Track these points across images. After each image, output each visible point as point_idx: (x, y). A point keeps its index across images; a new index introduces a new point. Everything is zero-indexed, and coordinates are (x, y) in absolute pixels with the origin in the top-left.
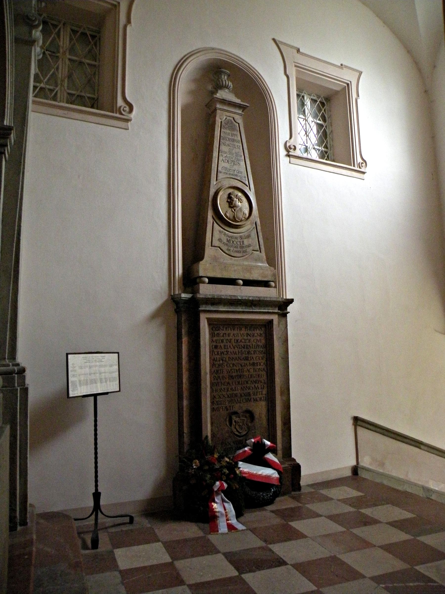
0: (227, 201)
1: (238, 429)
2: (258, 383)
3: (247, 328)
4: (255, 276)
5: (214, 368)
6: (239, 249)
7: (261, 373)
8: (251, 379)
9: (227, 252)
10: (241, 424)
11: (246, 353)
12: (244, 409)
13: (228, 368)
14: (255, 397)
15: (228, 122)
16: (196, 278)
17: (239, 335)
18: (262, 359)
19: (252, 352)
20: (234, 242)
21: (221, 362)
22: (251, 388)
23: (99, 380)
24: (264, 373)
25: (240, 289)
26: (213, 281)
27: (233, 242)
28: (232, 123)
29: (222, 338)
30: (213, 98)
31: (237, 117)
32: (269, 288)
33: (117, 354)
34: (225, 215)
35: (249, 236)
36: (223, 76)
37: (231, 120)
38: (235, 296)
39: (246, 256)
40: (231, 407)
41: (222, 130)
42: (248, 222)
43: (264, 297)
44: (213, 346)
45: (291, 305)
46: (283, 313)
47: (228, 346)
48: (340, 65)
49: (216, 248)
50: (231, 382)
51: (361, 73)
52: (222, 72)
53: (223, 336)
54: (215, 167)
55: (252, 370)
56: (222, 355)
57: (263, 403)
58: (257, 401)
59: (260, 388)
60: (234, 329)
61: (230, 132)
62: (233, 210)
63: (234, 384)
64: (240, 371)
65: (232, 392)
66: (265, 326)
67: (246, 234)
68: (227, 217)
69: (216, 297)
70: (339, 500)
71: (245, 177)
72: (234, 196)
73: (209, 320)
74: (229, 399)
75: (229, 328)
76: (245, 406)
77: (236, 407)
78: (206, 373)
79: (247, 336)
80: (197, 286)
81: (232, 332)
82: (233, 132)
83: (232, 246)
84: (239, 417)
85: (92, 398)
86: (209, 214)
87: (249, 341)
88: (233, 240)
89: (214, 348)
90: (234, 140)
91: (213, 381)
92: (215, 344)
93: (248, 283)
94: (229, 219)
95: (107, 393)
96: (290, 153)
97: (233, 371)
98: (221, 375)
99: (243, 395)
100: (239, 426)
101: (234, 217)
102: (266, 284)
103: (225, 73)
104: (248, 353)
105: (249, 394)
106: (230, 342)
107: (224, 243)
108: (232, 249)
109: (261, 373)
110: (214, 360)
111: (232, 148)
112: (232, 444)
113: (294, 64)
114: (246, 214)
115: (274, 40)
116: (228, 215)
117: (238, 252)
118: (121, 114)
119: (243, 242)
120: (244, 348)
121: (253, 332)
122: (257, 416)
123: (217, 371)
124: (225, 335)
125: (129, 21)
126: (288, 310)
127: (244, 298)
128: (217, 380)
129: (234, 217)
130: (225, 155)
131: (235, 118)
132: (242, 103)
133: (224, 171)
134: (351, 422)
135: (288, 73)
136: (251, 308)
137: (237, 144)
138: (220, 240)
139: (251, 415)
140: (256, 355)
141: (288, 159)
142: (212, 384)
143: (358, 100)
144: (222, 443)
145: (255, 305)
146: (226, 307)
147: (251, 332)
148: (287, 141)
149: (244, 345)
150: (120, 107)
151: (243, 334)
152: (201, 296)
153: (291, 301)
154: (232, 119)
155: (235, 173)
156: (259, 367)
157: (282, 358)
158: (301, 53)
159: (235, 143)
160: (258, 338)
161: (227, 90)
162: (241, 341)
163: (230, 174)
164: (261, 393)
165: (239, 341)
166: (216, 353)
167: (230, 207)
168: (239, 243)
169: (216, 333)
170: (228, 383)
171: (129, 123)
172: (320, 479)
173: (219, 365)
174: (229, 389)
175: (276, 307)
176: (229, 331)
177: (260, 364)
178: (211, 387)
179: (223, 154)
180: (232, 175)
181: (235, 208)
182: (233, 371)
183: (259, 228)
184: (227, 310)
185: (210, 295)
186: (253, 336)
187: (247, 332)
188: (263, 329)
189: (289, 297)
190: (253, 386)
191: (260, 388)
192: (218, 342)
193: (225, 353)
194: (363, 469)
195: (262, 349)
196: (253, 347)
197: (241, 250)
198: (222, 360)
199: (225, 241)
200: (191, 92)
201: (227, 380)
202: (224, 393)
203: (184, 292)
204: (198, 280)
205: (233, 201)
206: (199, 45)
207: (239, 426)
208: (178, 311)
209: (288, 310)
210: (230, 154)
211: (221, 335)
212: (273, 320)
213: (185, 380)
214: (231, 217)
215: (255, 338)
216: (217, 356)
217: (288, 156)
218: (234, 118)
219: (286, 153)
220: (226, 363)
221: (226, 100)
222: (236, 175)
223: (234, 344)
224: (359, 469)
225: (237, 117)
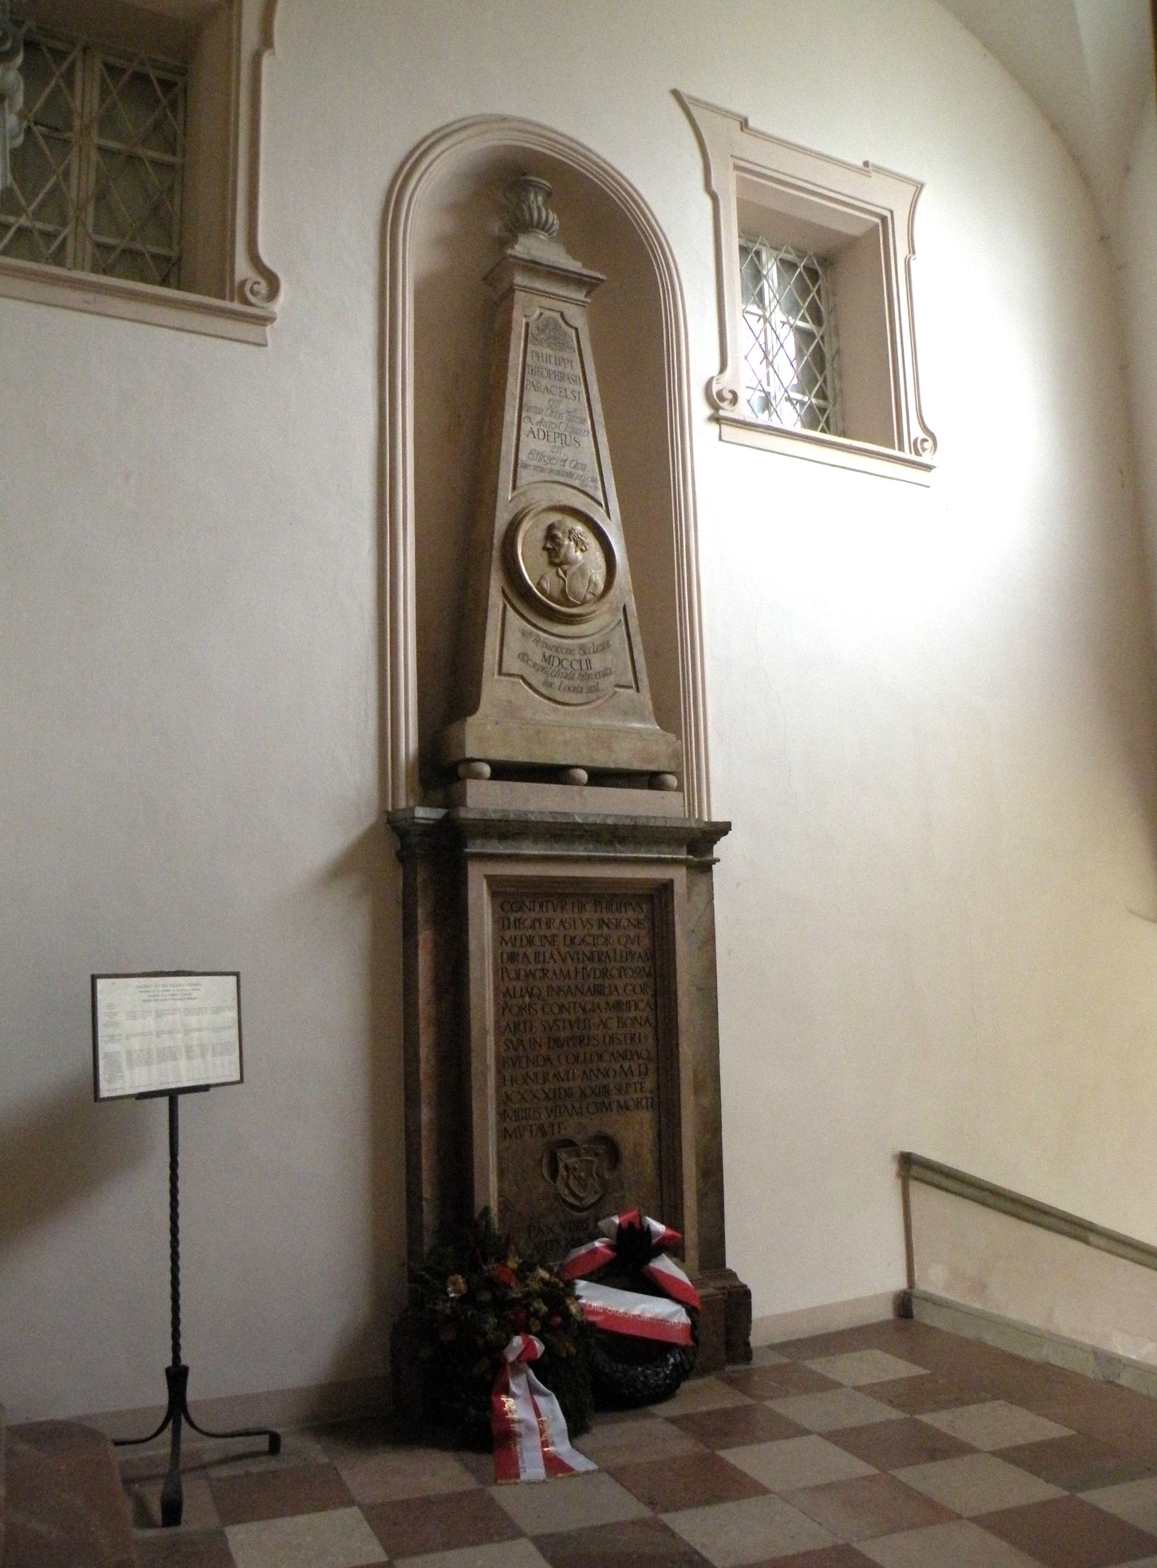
0: (545, 548)
1: (575, 1189)
2: (632, 1059)
3: (600, 903)
4: (623, 757)
6: (577, 683)
7: (639, 1030)
8: (611, 1048)
9: (543, 690)
10: (583, 1174)
11: (598, 973)
12: (592, 1131)
14: (622, 1099)
15: (546, 326)
16: (456, 764)
17: (579, 923)
18: (643, 991)
19: (615, 972)
20: (564, 663)
21: (527, 999)
22: (612, 1074)
23: (183, 1049)
24: (647, 1031)
26: (504, 771)
27: (560, 662)
28: (557, 327)
29: (530, 932)
30: (505, 258)
31: (571, 311)
32: (662, 793)
33: (234, 978)
34: (539, 585)
35: (604, 647)
36: (532, 197)
38: (566, 814)
39: (599, 702)
40: (556, 1128)
41: (529, 345)
42: (604, 606)
43: (648, 818)
44: (505, 956)
45: (723, 839)
46: (700, 862)
47: (547, 955)
48: (860, 164)
50: (553, 1057)
51: (920, 187)
52: (529, 183)
53: (533, 927)
54: (508, 452)
55: (613, 1024)
56: (531, 979)
57: (646, 1117)
58: (627, 1109)
59: (636, 1073)
60: (562, 908)
61: (551, 352)
62: (561, 573)
63: (563, 1062)
64: (582, 1026)
66: (650, 898)
67: (598, 639)
68: (543, 592)
69: (512, 817)
70: (858, 1389)
71: (594, 480)
72: (563, 533)
73: (492, 880)
74: (549, 1104)
75: (550, 905)
76: (593, 1124)
77: (570, 1128)
78: (485, 1032)
79: (600, 927)
80: (458, 785)
81: (558, 916)
84: (578, 1155)
85: (165, 1101)
86: (492, 582)
87: (607, 941)
88: (561, 657)
89: (506, 960)
90: (562, 377)
92: (509, 948)
93: (601, 777)
94: (550, 597)
95: (205, 1088)
96: (721, 413)
97: (561, 1025)
98: (526, 1038)
99: (588, 1092)
100: (578, 1179)
101: (563, 591)
102: (652, 780)
103: (538, 187)
105: (606, 1091)
106: (552, 943)
107: (535, 665)
108: (557, 681)
109: (639, 1030)
110: (507, 993)
111: (557, 398)
112: (557, 1230)
113: (731, 161)
114: (596, 585)
115: (676, 93)
116: (546, 586)
118: (246, 302)
119: (588, 661)
120: (591, 959)
121: (617, 915)
122: (627, 1152)
124: (537, 924)
125: (267, 40)
126: (715, 855)
127: (591, 820)
128: (516, 1050)
129: (563, 591)
130: (539, 418)
131: (566, 313)
132: (585, 272)
133: (535, 463)
134: (893, 1168)
136: (610, 849)
138: (523, 657)
139: (611, 1149)
140: (626, 981)
141: (715, 427)
142: (502, 1063)
143: (912, 262)
146: (539, 846)
147: (610, 915)
148: (712, 378)
149: (592, 953)
150: (243, 283)
151: (588, 920)
152: (471, 816)
153: (723, 829)
154: (557, 316)
155: (567, 468)
156: (633, 1014)
157: (700, 989)
158: (752, 130)
159: (566, 385)
160: (632, 933)
161: (542, 236)
162: (583, 941)
163: (551, 471)
164: (639, 1086)
165: (577, 940)
166: (513, 975)
167: (552, 564)
168: (576, 666)
169: (512, 919)
170: (547, 1059)
171: (268, 328)
172: (804, 1330)
173: (521, 1009)
174: (550, 1077)
175: (681, 845)
176: (551, 914)
178: (498, 1071)
179: (532, 415)
180: (558, 473)
181: (565, 567)
182: (561, 1025)
183: (634, 622)
184: (543, 852)
185: (495, 811)
186: (618, 926)
188: (645, 907)
189: (717, 817)
190: (617, 1067)
191: (636, 1073)
192: (518, 943)
193: (539, 974)
194: (926, 1300)
195: (641, 964)
196: (618, 956)
197: (582, 684)
198: (531, 995)
199: (538, 659)
200: (444, 242)
201: (544, 1051)
202: (535, 1088)
203: (424, 802)
204: (461, 770)
205: (560, 545)
206: (465, 108)
208: (405, 857)
209: (715, 855)
210: (551, 415)
211: (528, 923)
212: (672, 881)
213: (425, 1050)
214: (556, 593)
216: (514, 983)
217: (716, 419)
218: (562, 315)
219: (708, 412)
220: (540, 1004)
221: (540, 264)
222: (570, 475)
224: (913, 1299)
225: (571, 311)
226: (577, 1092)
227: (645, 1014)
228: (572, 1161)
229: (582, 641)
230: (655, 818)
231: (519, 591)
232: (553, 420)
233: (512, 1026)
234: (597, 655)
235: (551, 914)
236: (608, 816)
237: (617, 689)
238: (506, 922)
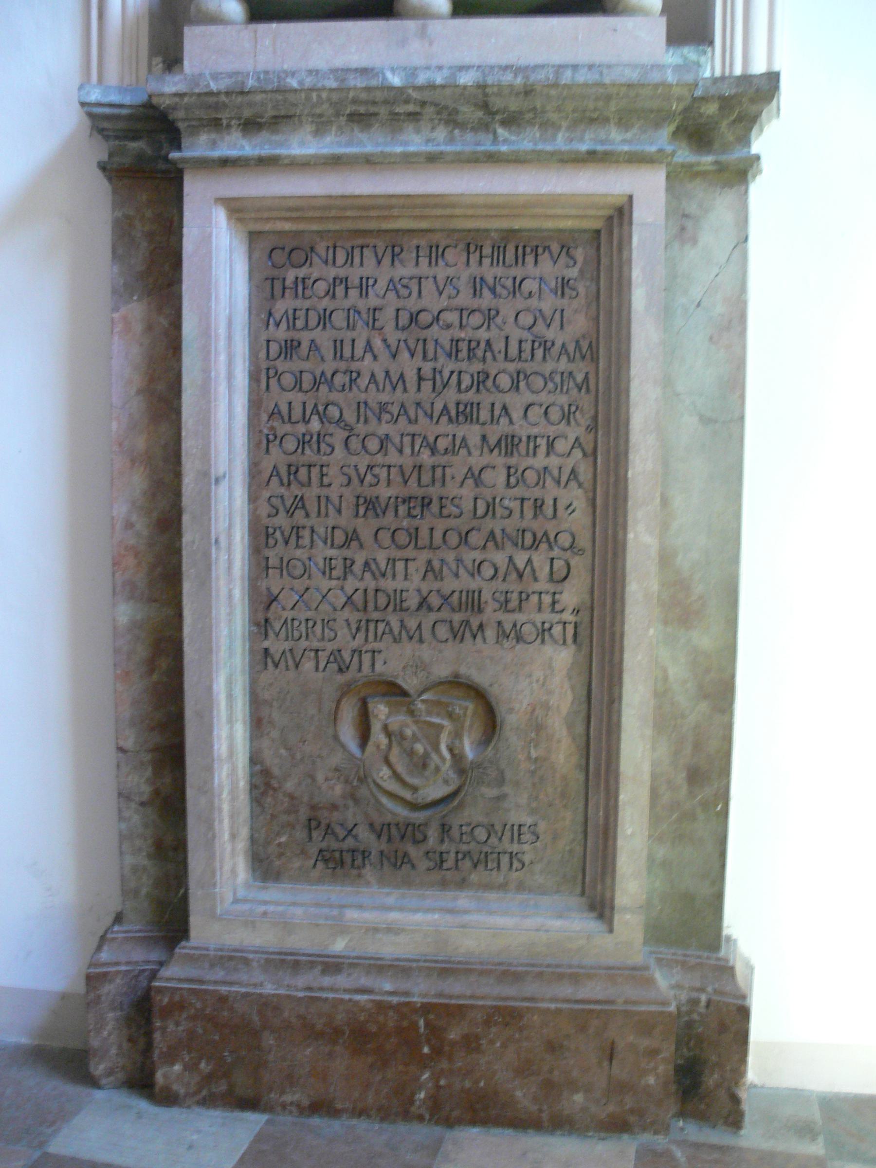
1: (400, 769)
2: (535, 545)
5: (276, 457)
8: (489, 524)
10: (419, 748)
12: (442, 671)
13: (354, 460)
14: (508, 620)
19: (504, 381)
21: (315, 425)
22: (488, 572)
24: (576, 496)
25: (423, 33)
29: (326, 303)
38: (364, 71)
43: (560, 68)
44: (274, 348)
50: (366, 535)
56: (324, 388)
57: (562, 657)
58: (519, 639)
64: (426, 478)
65: (370, 583)
69: (251, 83)
73: (236, 209)
76: (445, 659)
84: (411, 713)
87: (490, 316)
91: (266, 521)
92: (282, 333)
98: (312, 492)
99: (435, 601)
104: (481, 380)
106: (373, 324)
109: (551, 491)
112: (364, 834)
120: (453, 353)
122: (513, 719)
123: (293, 470)
124: (340, 290)
126: (755, 149)
127: (422, 79)
128: (290, 513)
140: (529, 397)
142: (261, 537)
144: (312, 824)
145: (512, 121)
147: (499, 271)
151: (449, 280)
156: (540, 461)
157: (705, 420)
160: (548, 304)
164: (547, 599)
165: (425, 318)
166: (288, 380)
169: (289, 282)
170: (352, 538)
174: (358, 568)
175: (657, 125)
176: (369, 268)
177: (550, 445)
182: (383, 474)
185: (215, 76)
187: (474, 269)
188: (579, 254)
189: (759, 67)
192: (300, 324)
195: (563, 365)
196: (513, 351)
201: (345, 520)
207: (411, 753)
211: (321, 286)
215: (520, 303)
216: (291, 396)
223: (393, 337)
226: (413, 602)
227: (570, 463)
228: (398, 720)
230: (575, 67)
233: (283, 471)
235: (369, 268)
236: (463, 68)
238: (278, 285)
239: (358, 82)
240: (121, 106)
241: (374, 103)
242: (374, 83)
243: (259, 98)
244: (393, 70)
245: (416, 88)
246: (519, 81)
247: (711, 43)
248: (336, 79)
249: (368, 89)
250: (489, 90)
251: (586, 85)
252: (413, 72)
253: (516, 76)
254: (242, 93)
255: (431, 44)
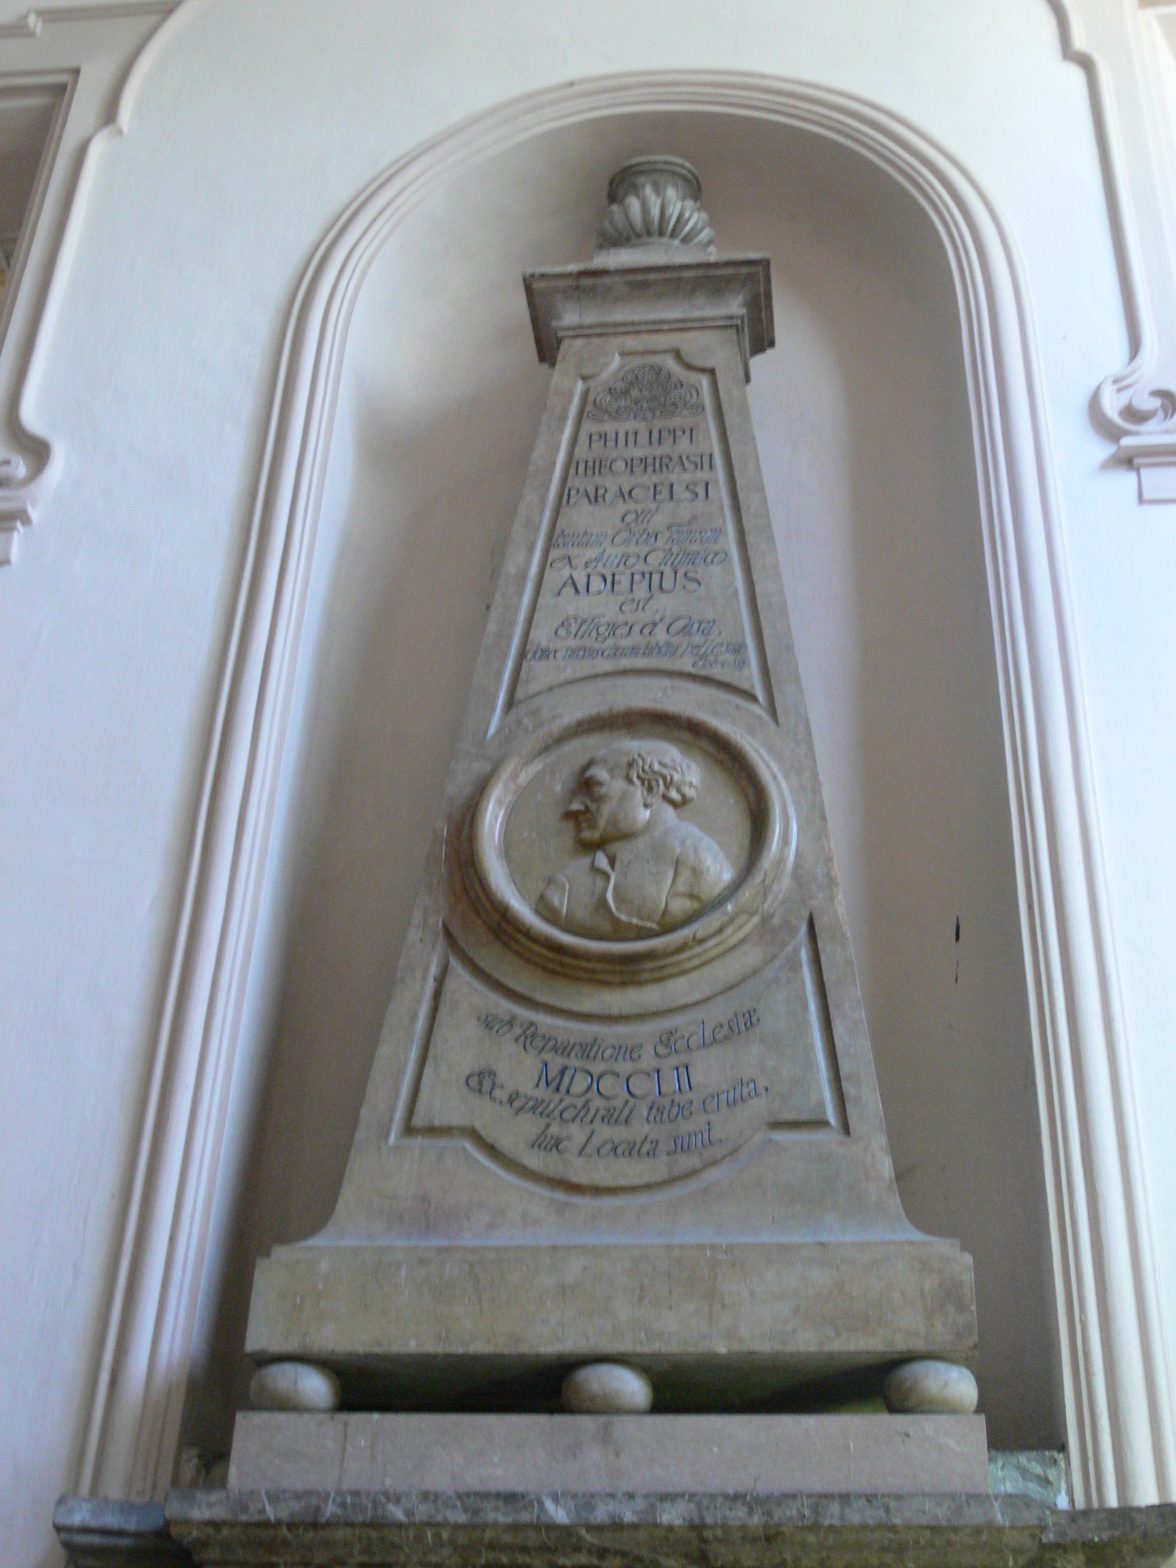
0: (569, 816)
4: (763, 1321)
6: (641, 1129)
9: (532, 1160)
25: (605, 1437)
26: (368, 1387)
31: (694, 344)
32: (899, 1420)
37: (657, 371)
38: (510, 1498)
39: (713, 1174)
43: (822, 1498)
49: (443, 1142)
61: (641, 426)
67: (717, 1013)
69: (330, 1510)
72: (611, 771)
82: (658, 424)
83: (582, 1114)
88: (597, 1068)
90: (663, 464)
93: (684, 1389)
94: (569, 928)
111: (653, 506)
116: (561, 902)
117: (632, 1150)
127: (601, 1513)
130: (591, 553)
131: (684, 349)
133: (572, 643)
135: (1080, 42)
137: (679, 478)
138: (481, 1081)
141: (1126, 480)
154: (670, 363)
155: (661, 635)
163: (617, 652)
179: (573, 552)
180: (634, 651)
181: (615, 847)
185: (275, 1497)
214: (583, 914)
217: (1127, 461)
218: (678, 355)
219: (1103, 450)
229: (665, 1024)
230: (845, 1498)
231: (478, 923)
232: (632, 549)
234: (714, 1051)
236: (665, 1497)
237: (779, 1136)
239: (499, 1516)
240: (120, 1533)
241: (524, 1549)
242: (525, 1517)
243: (340, 1534)
244: (556, 1499)
245: (590, 1528)
246: (756, 1520)
247: (1063, 1448)
248: (466, 1510)
249: (515, 1527)
250: (708, 1534)
251: (865, 1527)
252: (587, 1501)
253: (751, 1511)
254: (315, 1525)
255: (617, 1454)
